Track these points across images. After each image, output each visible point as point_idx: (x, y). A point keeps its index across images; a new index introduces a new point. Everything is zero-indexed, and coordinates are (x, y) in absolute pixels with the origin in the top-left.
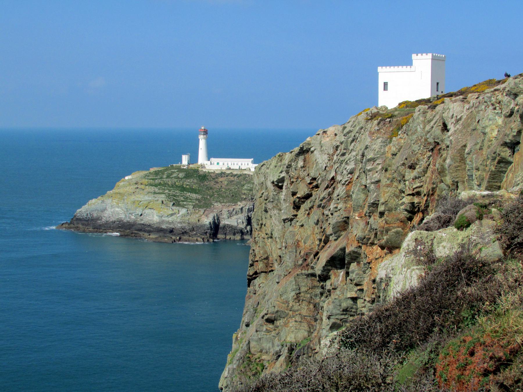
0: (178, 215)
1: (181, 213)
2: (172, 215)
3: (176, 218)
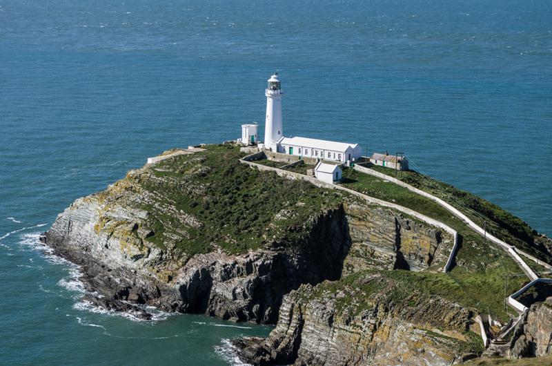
0: (146, 260)
1: (151, 256)
2: (136, 258)
3: (142, 265)
